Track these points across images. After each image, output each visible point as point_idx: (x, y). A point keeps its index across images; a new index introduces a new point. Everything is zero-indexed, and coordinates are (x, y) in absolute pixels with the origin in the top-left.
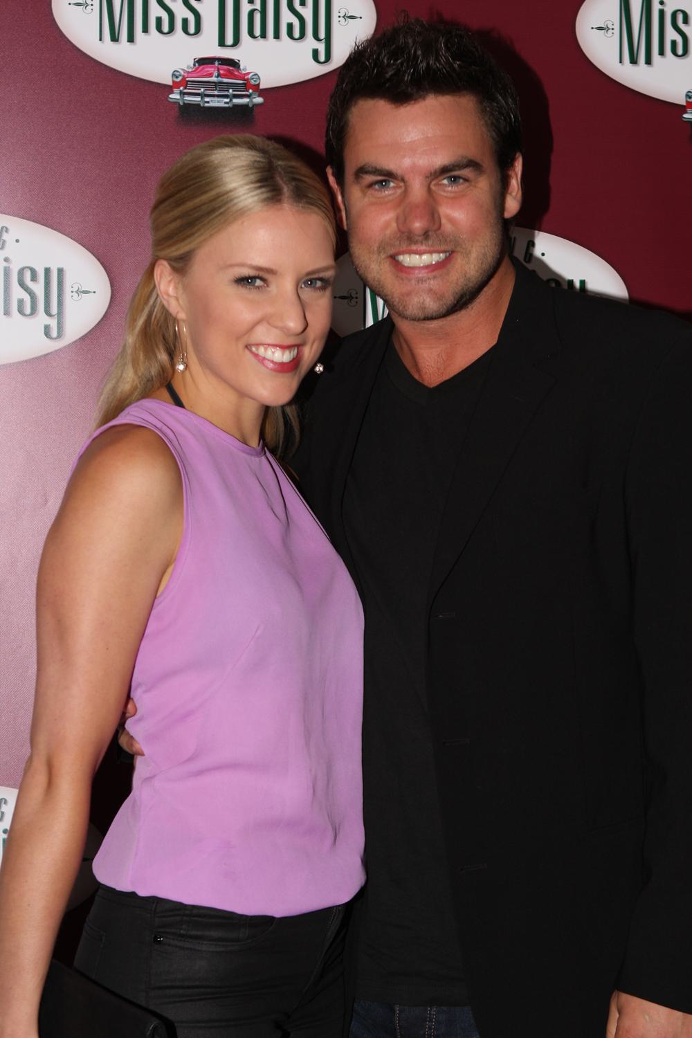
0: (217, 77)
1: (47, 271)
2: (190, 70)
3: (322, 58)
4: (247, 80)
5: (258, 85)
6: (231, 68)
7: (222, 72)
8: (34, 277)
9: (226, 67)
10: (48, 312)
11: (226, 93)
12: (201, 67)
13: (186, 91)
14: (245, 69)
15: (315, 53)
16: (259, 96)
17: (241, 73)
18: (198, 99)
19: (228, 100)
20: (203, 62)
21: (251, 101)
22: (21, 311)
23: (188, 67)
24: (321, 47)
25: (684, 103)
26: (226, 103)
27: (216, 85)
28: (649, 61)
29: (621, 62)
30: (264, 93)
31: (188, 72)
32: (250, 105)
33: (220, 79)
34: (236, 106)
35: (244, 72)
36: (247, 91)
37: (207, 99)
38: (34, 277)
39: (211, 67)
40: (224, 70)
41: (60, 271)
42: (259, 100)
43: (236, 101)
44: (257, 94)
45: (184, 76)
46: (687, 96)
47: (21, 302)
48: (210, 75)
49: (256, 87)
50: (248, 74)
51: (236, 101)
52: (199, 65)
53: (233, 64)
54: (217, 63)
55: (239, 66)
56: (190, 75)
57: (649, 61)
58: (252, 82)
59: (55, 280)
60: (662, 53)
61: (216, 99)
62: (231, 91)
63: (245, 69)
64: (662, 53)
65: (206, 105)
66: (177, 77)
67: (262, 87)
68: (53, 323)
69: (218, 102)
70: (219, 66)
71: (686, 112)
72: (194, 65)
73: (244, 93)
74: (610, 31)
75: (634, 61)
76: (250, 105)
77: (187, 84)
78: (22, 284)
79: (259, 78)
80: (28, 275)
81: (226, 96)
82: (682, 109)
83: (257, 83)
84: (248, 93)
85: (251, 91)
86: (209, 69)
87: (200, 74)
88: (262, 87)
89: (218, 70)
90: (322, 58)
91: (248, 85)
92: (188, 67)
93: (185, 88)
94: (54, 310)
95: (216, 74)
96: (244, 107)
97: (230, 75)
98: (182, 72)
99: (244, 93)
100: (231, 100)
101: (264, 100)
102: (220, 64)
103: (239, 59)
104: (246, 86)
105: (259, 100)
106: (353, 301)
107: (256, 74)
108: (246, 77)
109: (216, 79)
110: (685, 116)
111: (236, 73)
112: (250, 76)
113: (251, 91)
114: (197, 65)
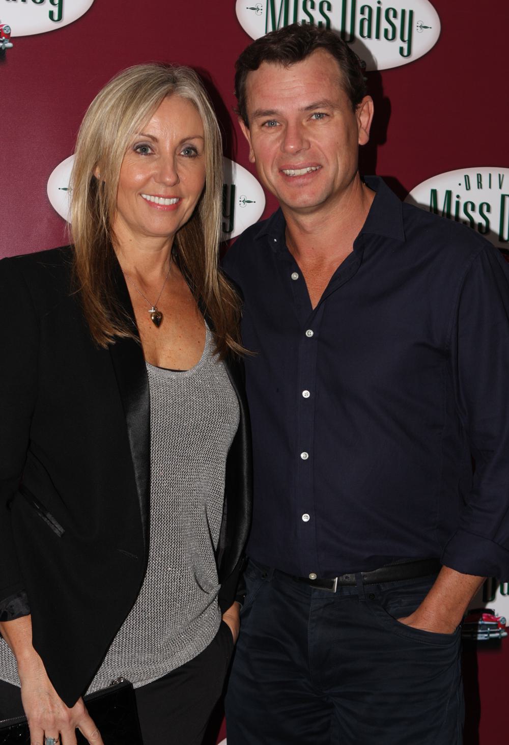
3: (56, 17)
15: (51, 14)
16: (10, 42)
21: (4, 45)
24: (56, 10)
30: (13, 40)
32: (3, 48)
42: (10, 45)
44: (8, 40)
67: (12, 35)
74: (260, 11)
76: (3, 48)
79: (10, 29)
83: (9, 32)
85: (4, 38)
88: (12, 35)
90: (56, 17)
105: (10, 45)
107: (8, 26)
113: (4, 38)
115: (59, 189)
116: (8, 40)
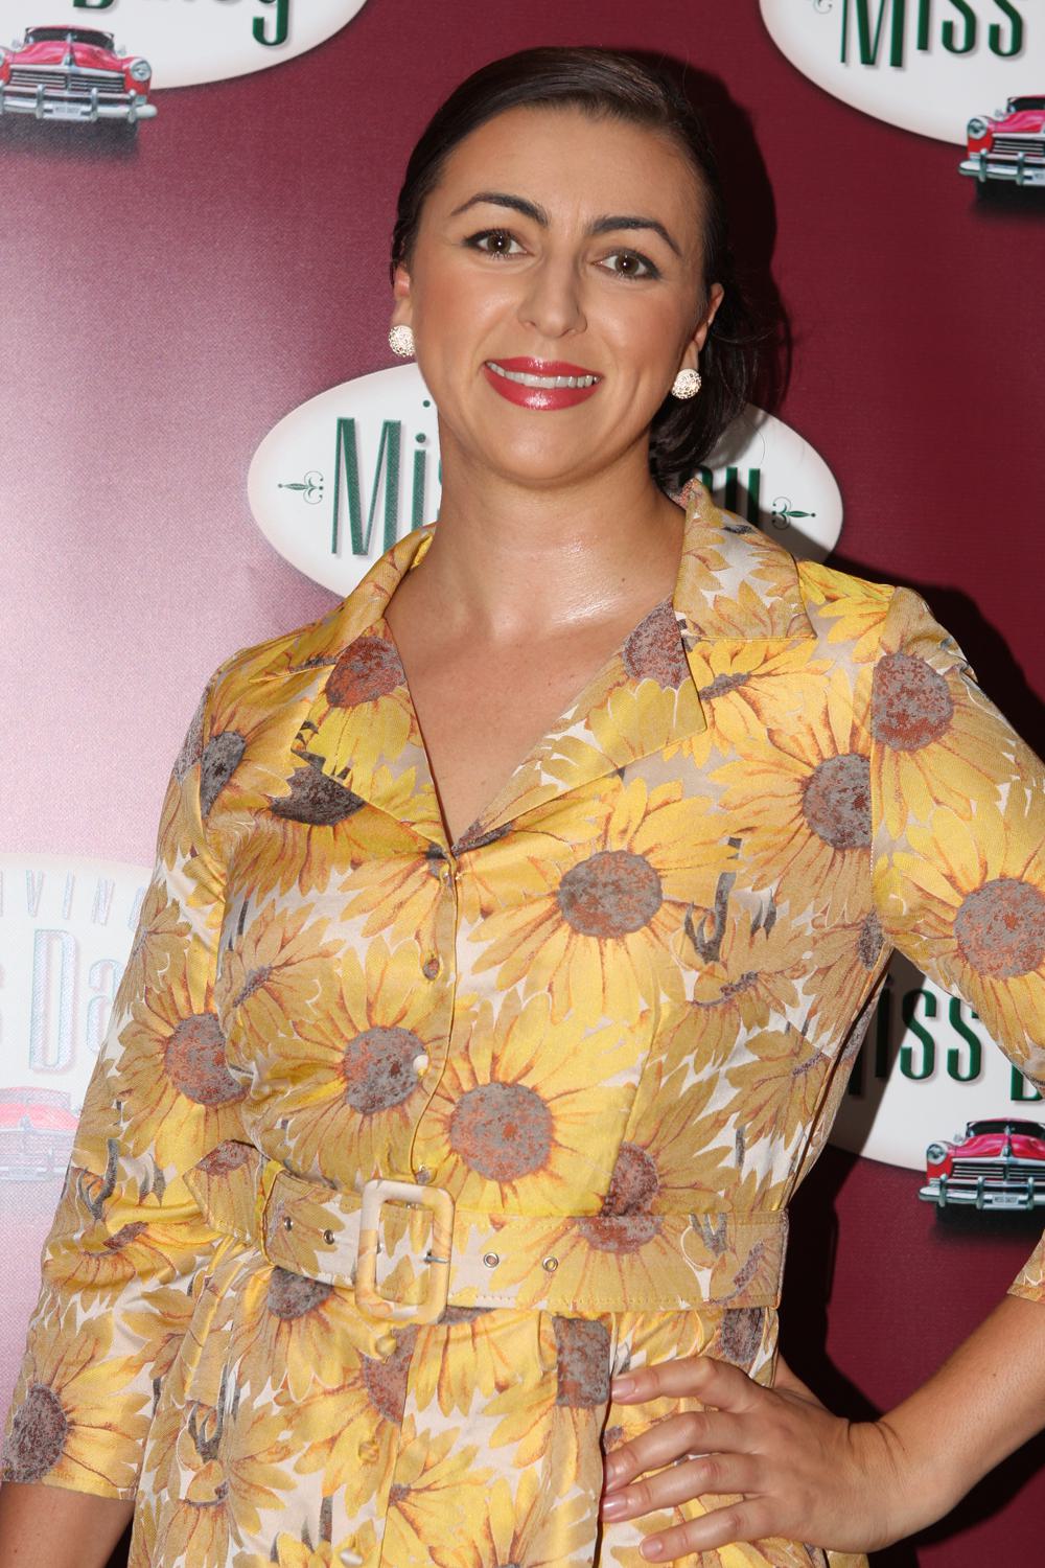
0: (70, 64)
3: (271, 34)
4: (127, 72)
5: (148, 82)
6: (97, 49)
7: (78, 55)
9: (85, 46)
11: (85, 95)
13: (8, 88)
14: (123, 51)
15: (259, 26)
16: (149, 102)
17: (113, 59)
18: (31, 104)
19: (87, 108)
20: (44, 35)
21: (133, 112)
24: (270, 14)
26: (84, 113)
27: (67, 78)
28: (897, 60)
30: (154, 96)
32: (131, 120)
33: (74, 68)
34: (103, 122)
35: (120, 57)
36: (126, 92)
37: (48, 105)
39: (58, 46)
40: (84, 52)
42: (148, 110)
43: (105, 111)
44: (145, 98)
45: (5, 61)
48: (57, 60)
49: (143, 87)
50: (128, 60)
51: (105, 111)
53: (99, 39)
55: (111, 46)
56: (17, 59)
57: (897, 60)
58: (136, 76)
60: (924, 44)
61: (66, 105)
62: (94, 91)
63: (123, 51)
64: (924, 44)
65: (47, 116)
67: (154, 85)
69: (70, 111)
73: (119, 96)
75: (868, 59)
76: (131, 120)
77: (11, 76)
79: (150, 70)
81: (87, 101)
82: (961, 152)
83: (145, 78)
84: (126, 97)
85: (132, 93)
86: (55, 49)
87: (36, 57)
88: (154, 85)
89: (72, 51)
90: (271, 34)
91: (127, 82)
92: (15, 43)
93: (8, 84)
95: (67, 58)
96: (119, 124)
97: (93, 61)
99: (119, 96)
100: (94, 109)
101: (160, 110)
102: (75, 40)
103: (113, 32)
104: (124, 83)
105: (148, 110)
106: (316, 492)
107: (143, 62)
108: (125, 67)
109: (66, 67)
111: (106, 58)
112: (131, 65)
113: (132, 93)
114: (31, 40)
115: (280, 486)
116: (145, 98)
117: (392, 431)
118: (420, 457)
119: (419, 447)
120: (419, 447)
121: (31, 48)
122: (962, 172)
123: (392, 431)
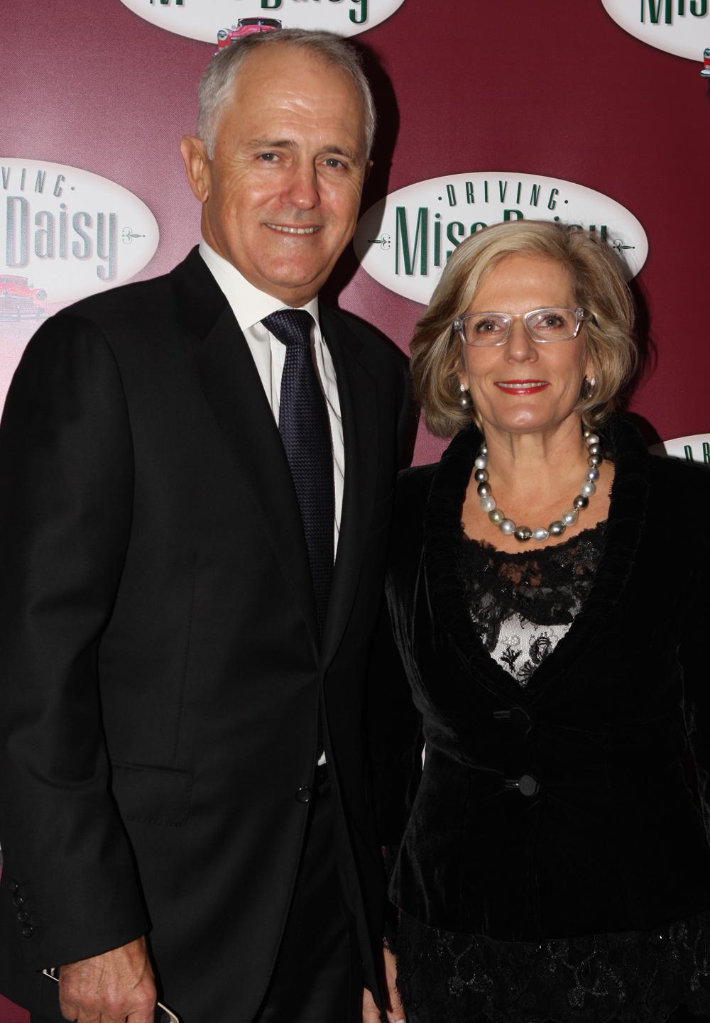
1: (101, 216)
2: (235, 30)
3: (359, 18)
8: (88, 223)
10: (101, 255)
12: (245, 28)
15: (352, 13)
20: (246, 22)
22: (76, 253)
23: (233, 27)
24: (358, 8)
25: (702, 60)
28: (669, 20)
29: (642, 21)
31: (233, 32)
38: (88, 223)
39: (254, 27)
41: (113, 218)
46: (705, 53)
47: (76, 245)
52: (244, 25)
54: (259, 23)
57: (669, 21)
59: (106, 223)
60: (681, 12)
64: (681, 12)
66: (222, 37)
68: (106, 264)
70: (262, 26)
71: (704, 69)
72: (239, 25)
75: (655, 20)
78: (77, 229)
80: (83, 220)
82: (701, 66)
90: (359, 18)
94: (107, 253)
98: (227, 32)
106: (387, 244)
110: (703, 72)
114: (241, 25)
117: (423, 213)
118: (438, 226)
119: (437, 220)
120: (437, 220)
121: (241, 29)
122: (702, 75)
123: (423, 213)
